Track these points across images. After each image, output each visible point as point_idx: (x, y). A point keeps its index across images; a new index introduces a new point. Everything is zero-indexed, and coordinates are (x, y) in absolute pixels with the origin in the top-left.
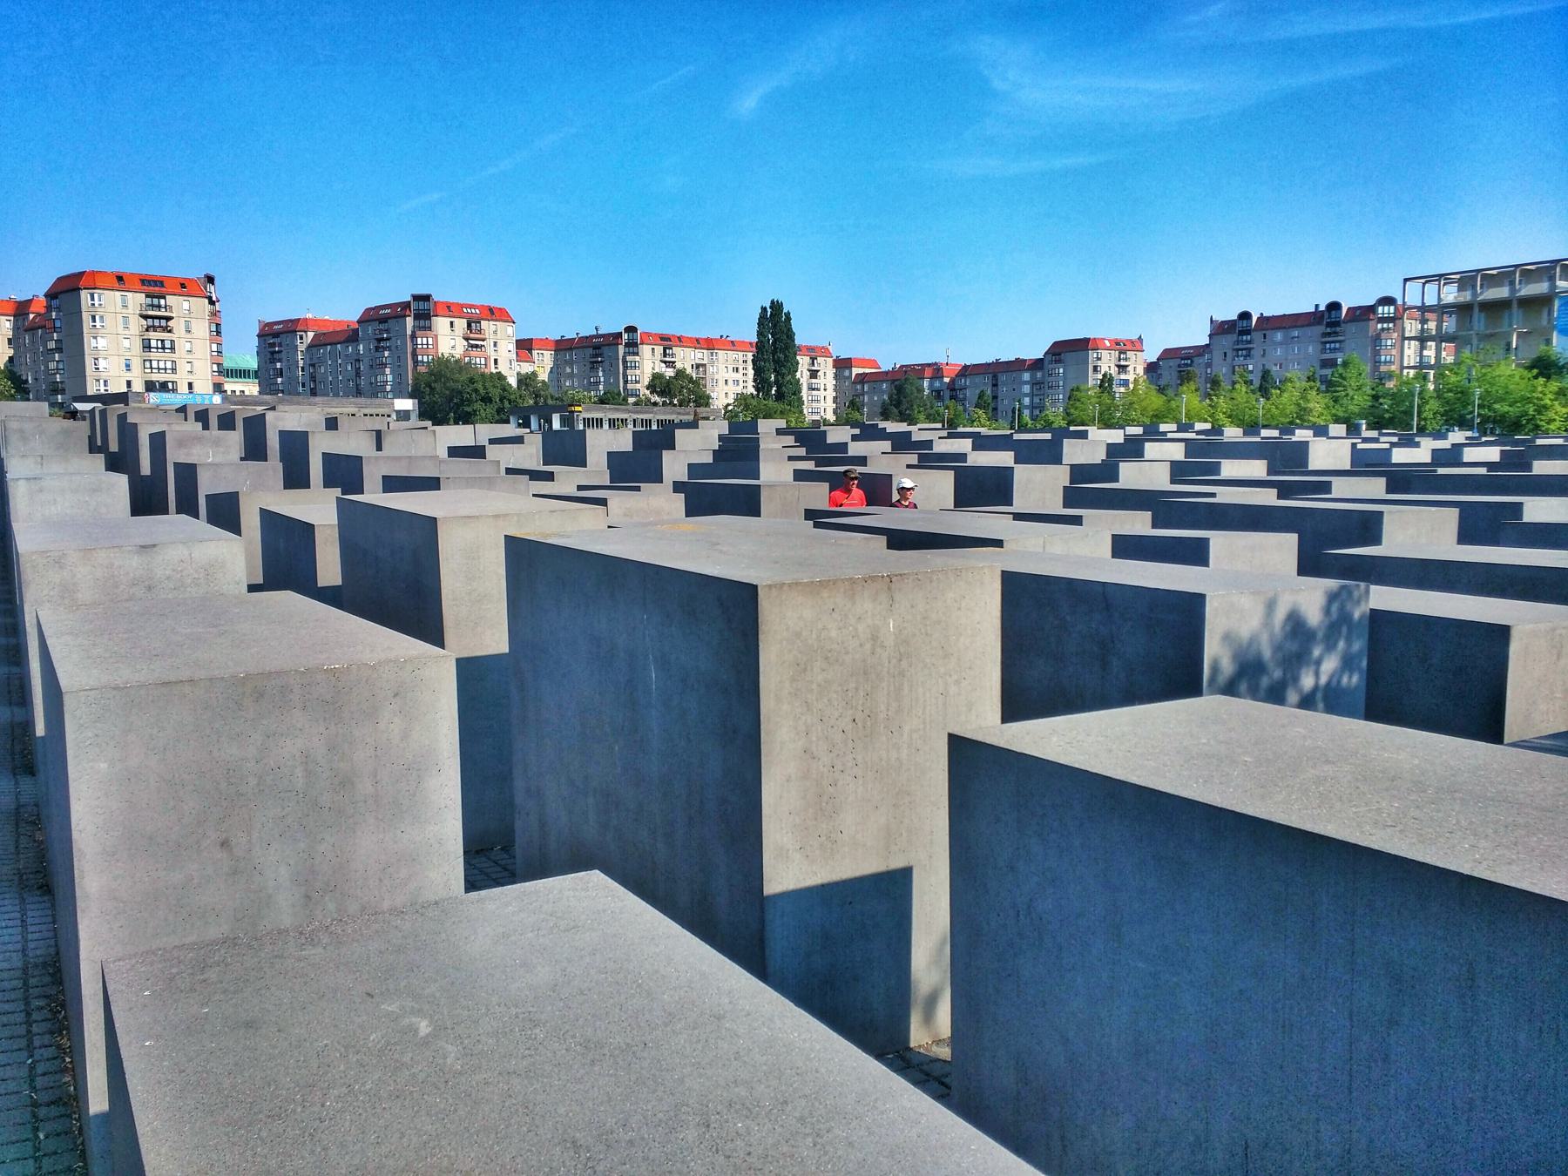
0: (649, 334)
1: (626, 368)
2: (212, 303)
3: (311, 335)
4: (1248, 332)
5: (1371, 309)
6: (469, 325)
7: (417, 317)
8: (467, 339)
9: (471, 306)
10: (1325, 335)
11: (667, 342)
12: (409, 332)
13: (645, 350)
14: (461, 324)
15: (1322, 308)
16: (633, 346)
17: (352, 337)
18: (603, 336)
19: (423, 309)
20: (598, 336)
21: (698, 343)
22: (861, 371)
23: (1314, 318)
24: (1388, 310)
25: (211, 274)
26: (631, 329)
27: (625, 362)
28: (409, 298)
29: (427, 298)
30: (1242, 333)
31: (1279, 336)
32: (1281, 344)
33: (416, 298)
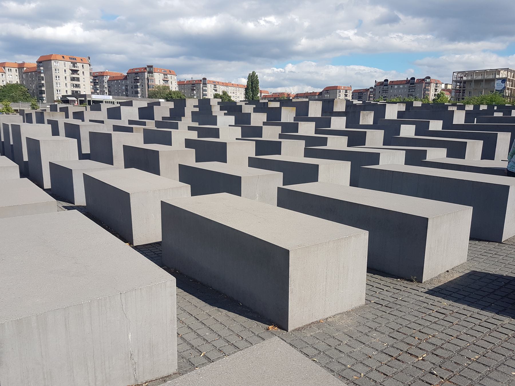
0: (210, 81)
1: (203, 91)
3: (108, 77)
4: (387, 85)
5: (424, 80)
10: (409, 87)
12: (146, 77)
13: (209, 85)
15: (409, 79)
16: (205, 84)
17: (126, 78)
18: (194, 81)
19: (150, 69)
21: (223, 84)
22: (264, 94)
23: (407, 82)
24: (428, 80)
27: (203, 89)
29: (152, 67)
30: (385, 86)
31: (396, 87)
32: (396, 89)
33: (148, 66)
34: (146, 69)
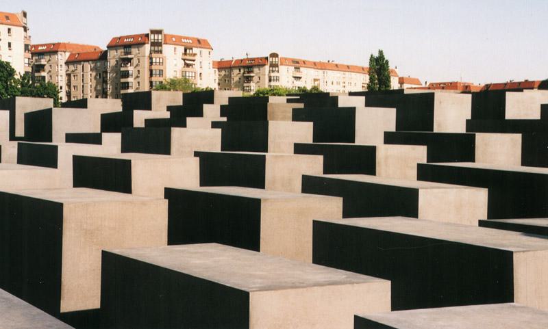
0: (286, 59)
2: (25, 29)
6: (185, 50)
7: (153, 44)
8: (184, 60)
9: (187, 38)
11: (297, 64)
14: (181, 49)
19: (155, 40)
20: (249, 60)
21: (316, 65)
25: (26, 10)
26: (274, 55)
28: (148, 32)
29: (159, 32)
33: (153, 32)
34: (147, 35)
